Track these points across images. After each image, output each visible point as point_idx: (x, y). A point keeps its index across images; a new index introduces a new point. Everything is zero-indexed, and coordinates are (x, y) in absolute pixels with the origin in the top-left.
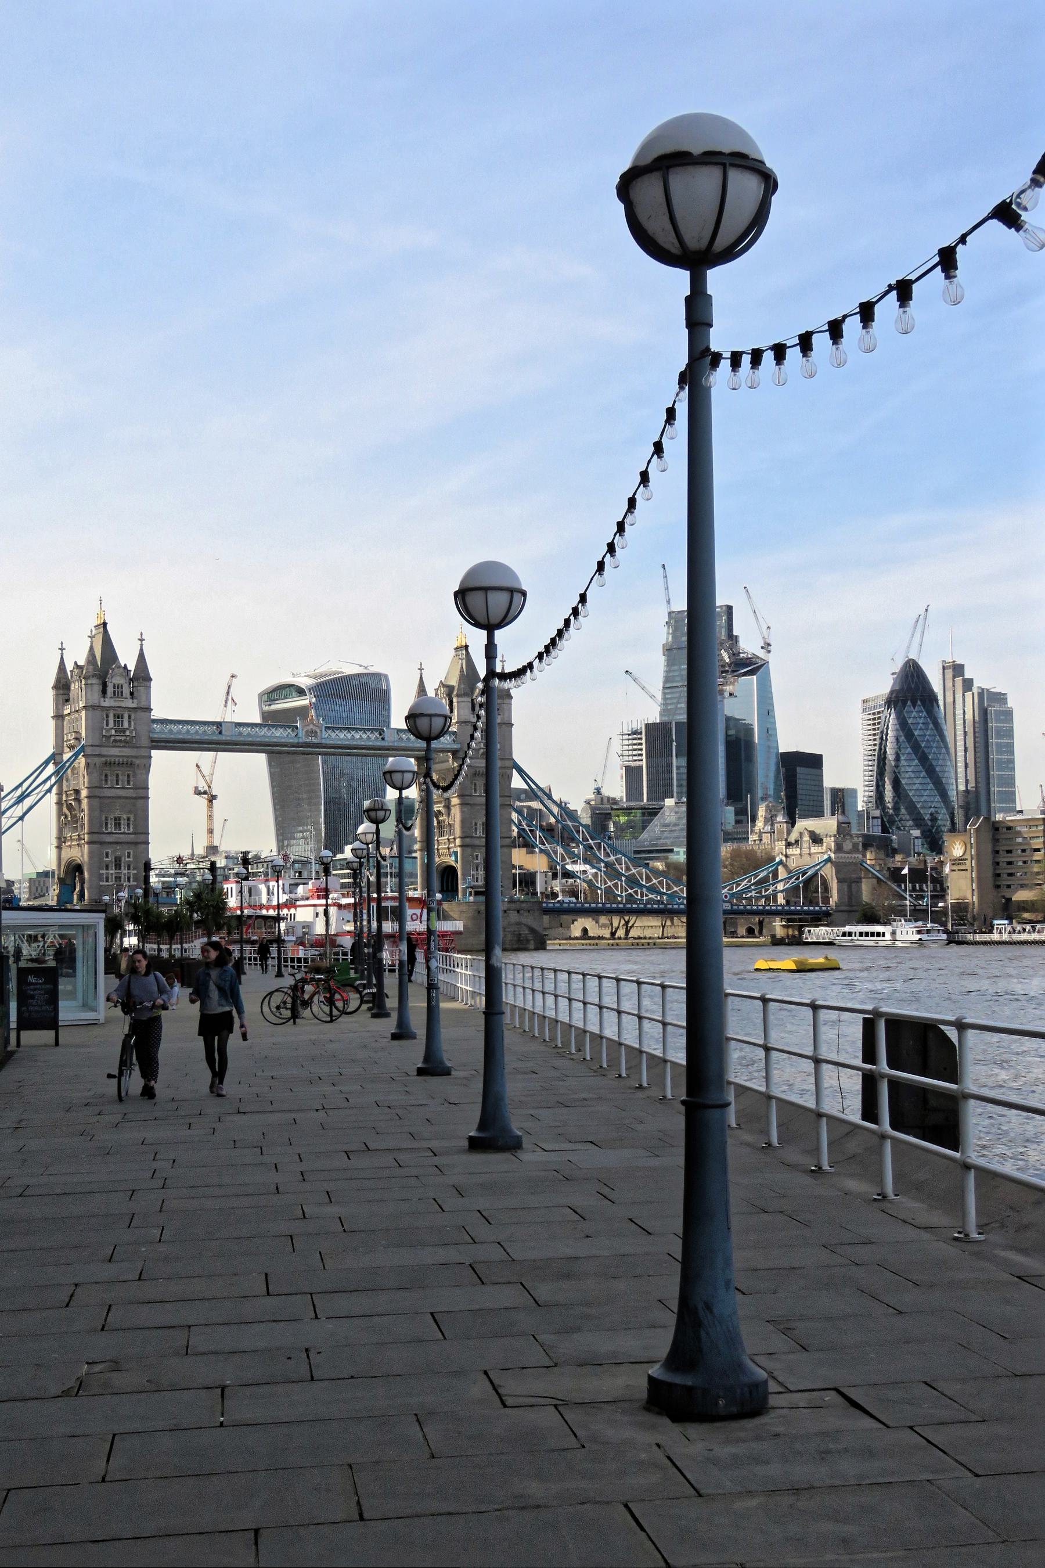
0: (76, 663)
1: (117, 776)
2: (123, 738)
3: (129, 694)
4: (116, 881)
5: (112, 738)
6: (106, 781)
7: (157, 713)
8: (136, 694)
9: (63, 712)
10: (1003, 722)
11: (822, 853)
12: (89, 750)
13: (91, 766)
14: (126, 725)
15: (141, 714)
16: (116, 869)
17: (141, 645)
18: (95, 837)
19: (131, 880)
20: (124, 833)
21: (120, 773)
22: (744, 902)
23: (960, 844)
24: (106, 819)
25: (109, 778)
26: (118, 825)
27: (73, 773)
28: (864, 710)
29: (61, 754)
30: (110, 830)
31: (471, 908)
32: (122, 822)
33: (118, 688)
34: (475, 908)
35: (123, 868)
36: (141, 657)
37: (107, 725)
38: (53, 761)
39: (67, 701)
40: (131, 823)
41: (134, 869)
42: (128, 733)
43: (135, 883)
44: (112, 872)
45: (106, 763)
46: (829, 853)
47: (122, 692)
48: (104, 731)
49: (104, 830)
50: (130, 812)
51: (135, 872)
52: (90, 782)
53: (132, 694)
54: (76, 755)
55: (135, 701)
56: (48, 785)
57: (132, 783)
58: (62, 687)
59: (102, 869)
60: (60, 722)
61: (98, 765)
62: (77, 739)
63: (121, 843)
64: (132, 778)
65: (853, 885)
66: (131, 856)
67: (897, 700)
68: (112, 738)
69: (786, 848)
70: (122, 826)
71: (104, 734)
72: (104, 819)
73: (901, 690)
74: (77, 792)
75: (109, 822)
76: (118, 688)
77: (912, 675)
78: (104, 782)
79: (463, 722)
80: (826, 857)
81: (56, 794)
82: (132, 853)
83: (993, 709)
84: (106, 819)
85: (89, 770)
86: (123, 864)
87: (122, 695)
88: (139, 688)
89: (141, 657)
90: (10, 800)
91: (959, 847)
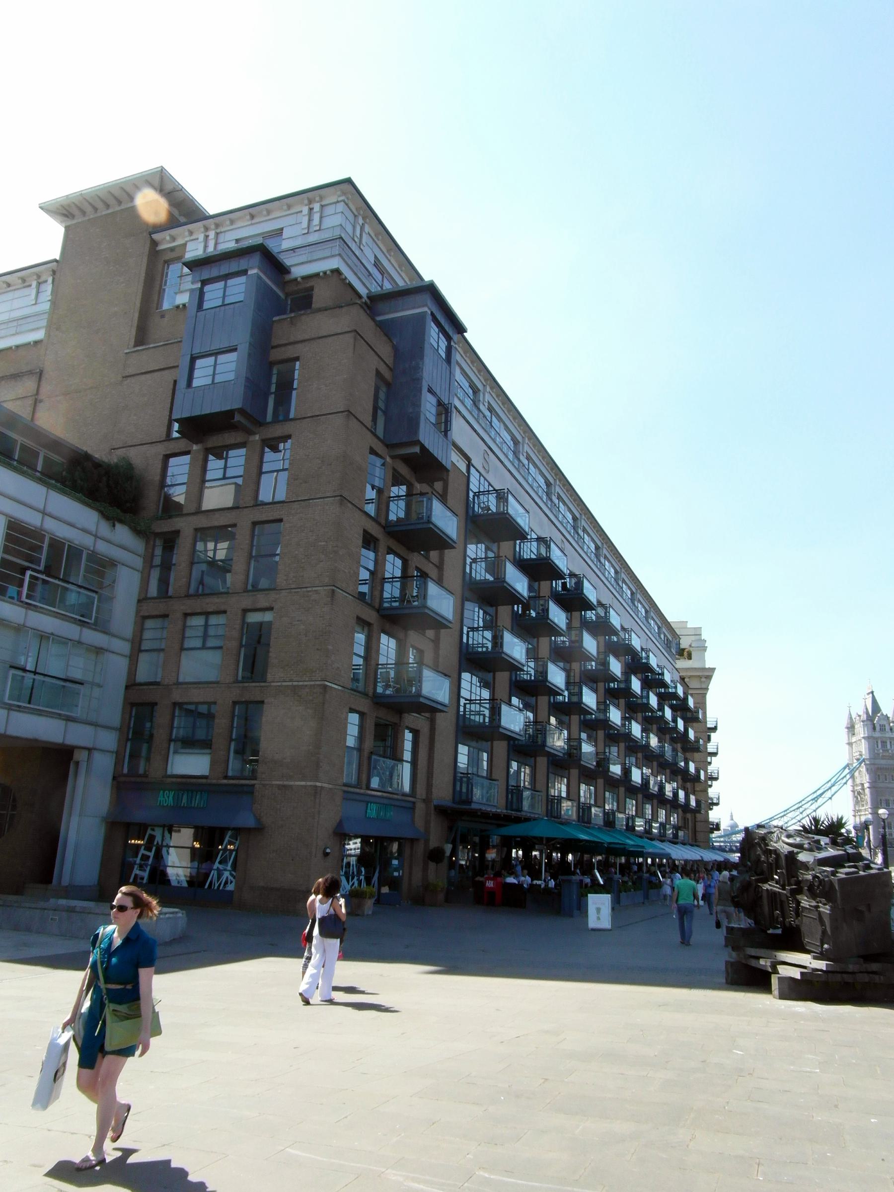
0: (857, 714)
1: (886, 776)
2: (888, 754)
5: (881, 755)
6: (879, 779)
14: (889, 746)
24: (881, 800)
25: (881, 777)
27: (859, 774)
29: (852, 764)
32: (890, 802)
37: (877, 747)
39: (854, 734)
42: (890, 751)
54: (861, 763)
56: (844, 780)
58: (851, 728)
62: (861, 755)
74: (862, 785)
75: (883, 801)
81: (477, 742)
84: (881, 800)
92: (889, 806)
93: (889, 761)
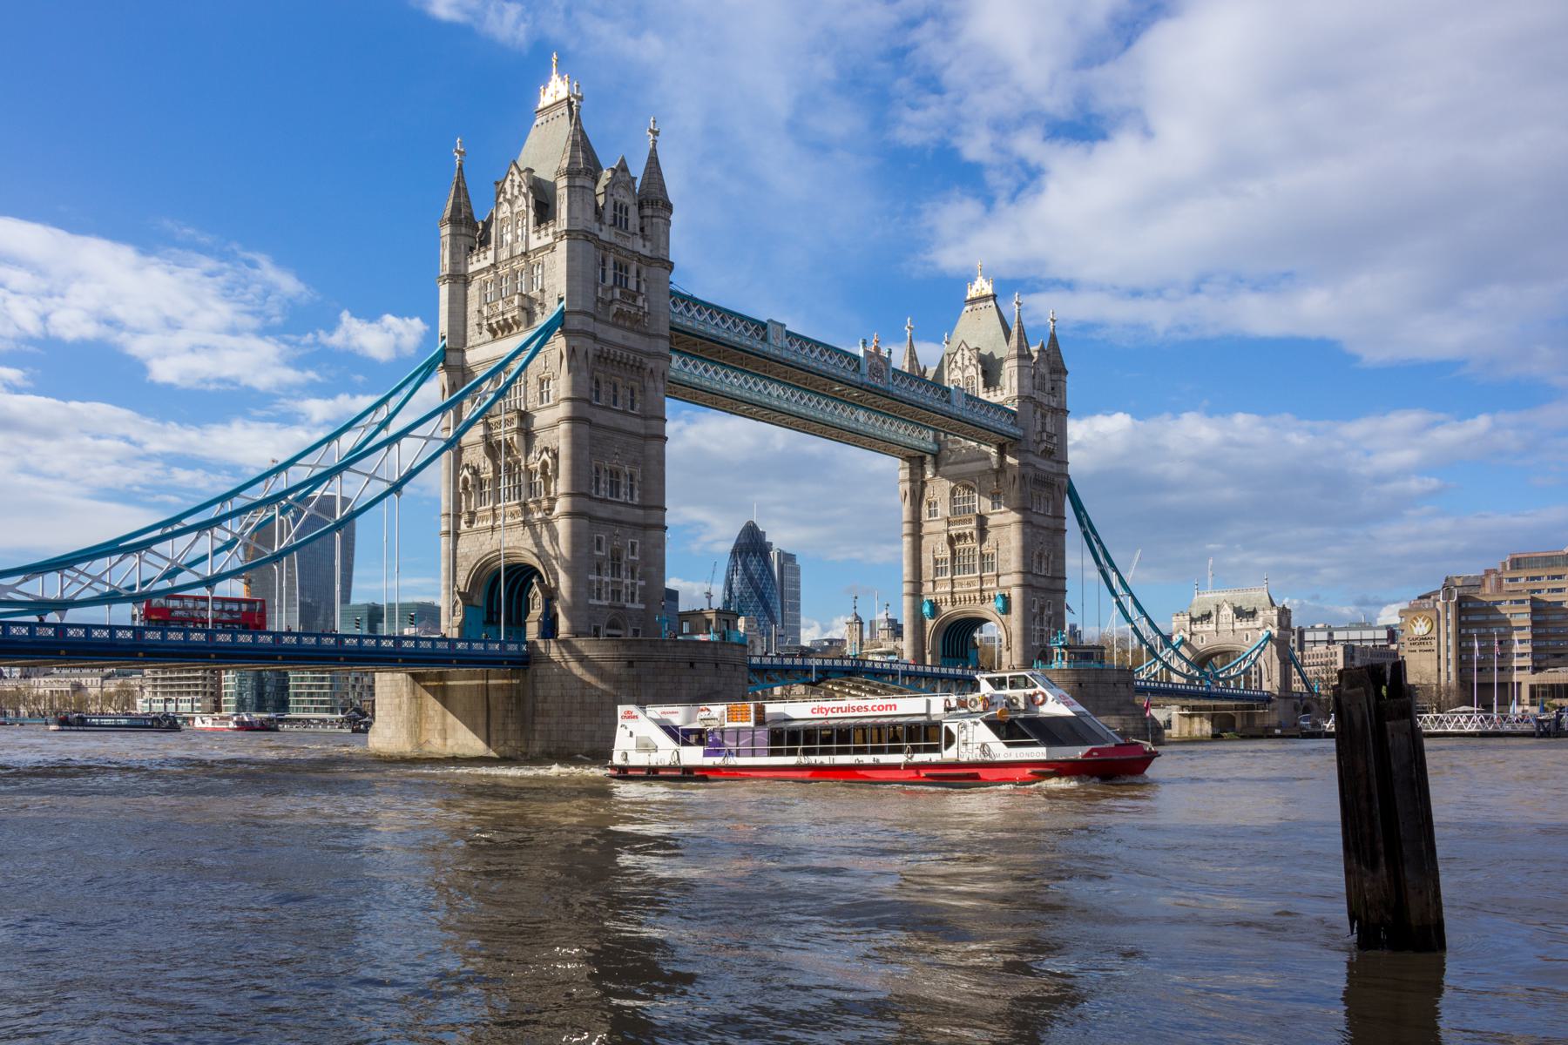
3: (638, 230)
4: (613, 600)
5: (614, 308)
6: (597, 393)
8: (648, 231)
12: (574, 322)
13: (580, 354)
14: (632, 285)
15: (658, 271)
16: (613, 576)
18: (585, 505)
19: (637, 599)
20: (625, 504)
21: (620, 381)
23: (1423, 620)
24: (598, 471)
25: (603, 387)
26: (615, 487)
30: (602, 494)
32: (623, 481)
33: (621, 212)
35: (623, 573)
37: (604, 281)
38: (441, 365)
40: (636, 485)
42: (640, 302)
43: (642, 606)
44: (607, 579)
45: (599, 357)
46: (1269, 628)
47: (627, 220)
48: (600, 289)
49: (593, 491)
50: (635, 463)
51: (643, 583)
52: (575, 386)
53: (642, 229)
55: (648, 244)
57: (638, 406)
60: (459, 287)
64: (638, 397)
66: (637, 550)
68: (614, 308)
70: (622, 490)
71: (600, 294)
76: (621, 212)
79: (1027, 397)
80: (1263, 634)
82: (638, 546)
84: (598, 471)
86: (624, 566)
87: (627, 227)
88: (655, 220)
91: (1423, 624)
92: (618, 496)
93: (632, 336)
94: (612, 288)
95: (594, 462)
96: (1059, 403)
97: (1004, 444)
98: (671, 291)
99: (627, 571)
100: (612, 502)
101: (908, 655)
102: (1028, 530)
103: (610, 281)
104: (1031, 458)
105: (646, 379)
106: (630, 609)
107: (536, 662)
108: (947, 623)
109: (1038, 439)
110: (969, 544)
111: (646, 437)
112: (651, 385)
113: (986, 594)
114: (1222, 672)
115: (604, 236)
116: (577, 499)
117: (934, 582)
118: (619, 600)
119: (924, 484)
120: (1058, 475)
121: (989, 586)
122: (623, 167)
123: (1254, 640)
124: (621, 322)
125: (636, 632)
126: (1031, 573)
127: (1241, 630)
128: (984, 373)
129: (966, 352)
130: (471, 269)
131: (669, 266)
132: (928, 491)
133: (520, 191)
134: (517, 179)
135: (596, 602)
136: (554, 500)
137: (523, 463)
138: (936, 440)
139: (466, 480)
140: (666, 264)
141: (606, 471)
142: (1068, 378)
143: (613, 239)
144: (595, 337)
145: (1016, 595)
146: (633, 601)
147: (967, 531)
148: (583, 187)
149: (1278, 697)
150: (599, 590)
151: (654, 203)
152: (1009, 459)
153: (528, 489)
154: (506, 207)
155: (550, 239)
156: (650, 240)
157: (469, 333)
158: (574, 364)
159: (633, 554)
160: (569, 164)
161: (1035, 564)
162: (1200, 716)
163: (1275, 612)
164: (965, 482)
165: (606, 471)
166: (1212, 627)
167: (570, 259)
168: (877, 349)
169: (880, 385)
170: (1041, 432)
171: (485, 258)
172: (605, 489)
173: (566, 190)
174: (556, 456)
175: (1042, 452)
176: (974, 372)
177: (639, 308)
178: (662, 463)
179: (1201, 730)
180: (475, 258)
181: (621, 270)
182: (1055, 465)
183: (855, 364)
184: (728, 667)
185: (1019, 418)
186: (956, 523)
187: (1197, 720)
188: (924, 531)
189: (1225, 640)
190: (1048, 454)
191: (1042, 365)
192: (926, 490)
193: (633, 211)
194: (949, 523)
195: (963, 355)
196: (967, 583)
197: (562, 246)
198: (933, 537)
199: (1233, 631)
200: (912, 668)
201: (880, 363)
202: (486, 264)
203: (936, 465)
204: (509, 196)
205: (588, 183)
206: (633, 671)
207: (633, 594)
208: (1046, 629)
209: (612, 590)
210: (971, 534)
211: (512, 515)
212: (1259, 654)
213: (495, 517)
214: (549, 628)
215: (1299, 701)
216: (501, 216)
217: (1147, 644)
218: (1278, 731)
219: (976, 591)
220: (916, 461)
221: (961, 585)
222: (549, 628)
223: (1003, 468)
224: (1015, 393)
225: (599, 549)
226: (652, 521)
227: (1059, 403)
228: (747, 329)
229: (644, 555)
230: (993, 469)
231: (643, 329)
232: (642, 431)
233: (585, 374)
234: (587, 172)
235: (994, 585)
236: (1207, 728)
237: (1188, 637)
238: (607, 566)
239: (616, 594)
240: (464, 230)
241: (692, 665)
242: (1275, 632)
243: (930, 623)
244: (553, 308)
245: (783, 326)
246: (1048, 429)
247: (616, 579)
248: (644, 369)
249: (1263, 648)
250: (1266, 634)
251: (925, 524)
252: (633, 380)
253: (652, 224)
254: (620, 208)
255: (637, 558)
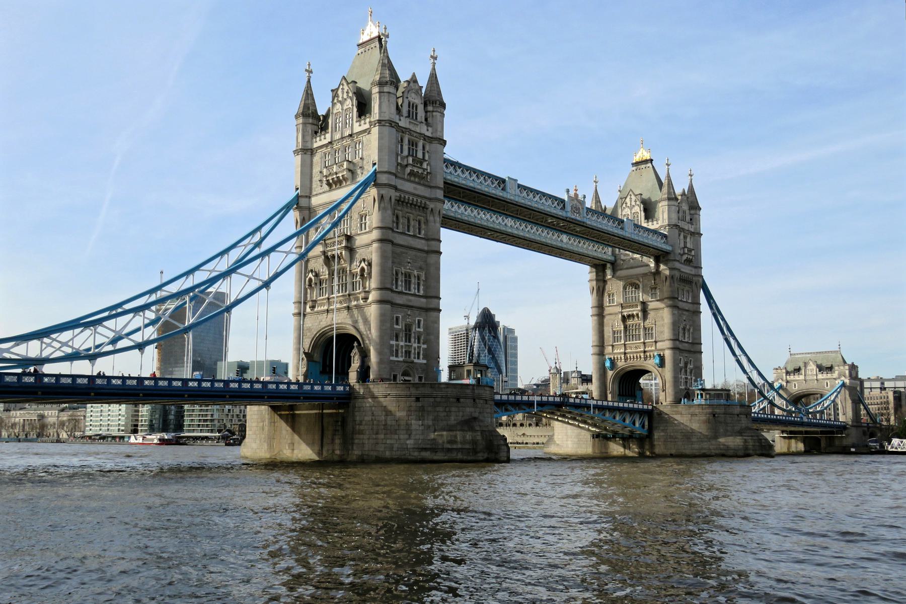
4: (406, 357)
5: (408, 170)
6: (397, 224)
7: (450, 152)
8: (430, 120)
9: (312, 144)
10: (513, 342)
11: (834, 379)
12: (383, 179)
13: (387, 199)
14: (420, 155)
15: (436, 146)
16: (406, 341)
17: (434, 64)
18: (389, 296)
19: (421, 356)
20: (414, 295)
22: (810, 416)
24: (397, 274)
25: (401, 220)
26: (408, 283)
28: (450, 333)
31: (705, 411)
32: (413, 280)
33: (413, 108)
34: (710, 411)
35: (413, 340)
36: (433, 78)
37: (402, 152)
38: (295, 206)
40: (422, 283)
41: (423, 344)
42: (425, 165)
43: (425, 362)
45: (398, 201)
46: (843, 378)
47: (416, 114)
48: (399, 158)
49: (394, 287)
50: (421, 268)
51: (425, 346)
52: (383, 219)
53: (426, 120)
55: (430, 129)
57: (423, 232)
59: (393, 340)
60: (308, 156)
61: (393, 200)
63: (412, 307)
64: (423, 226)
65: (857, 405)
66: (422, 325)
67: (480, 326)
68: (408, 170)
69: (786, 375)
70: (412, 286)
71: (399, 161)
72: (394, 272)
73: (482, 322)
76: (413, 108)
77: (487, 316)
78: (395, 225)
80: (839, 382)
82: (422, 323)
83: (509, 336)
84: (397, 274)
85: (382, 205)
86: (413, 335)
87: (416, 118)
88: (434, 113)
89: (433, 78)
90: (245, 246)
92: (410, 290)
93: (418, 187)
94: (407, 157)
95: (395, 268)
96: (695, 229)
97: (659, 256)
98: (445, 159)
99: (415, 338)
100: (406, 294)
101: (595, 394)
102: (676, 312)
103: (406, 153)
104: (677, 265)
105: (428, 215)
106: (416, 363)
107: (356, 398)
108: (622, 373)
109: (682, 252)
110: (636, 321)
111: (427, 252)
112: (431, 218)
113: (648, 354)
114: (811, 408)
115: (402, 124)
116: (384, 292)
117: (613, 346)
118: (410, 357)
119: (605, 282)
120: (695, 275)
121: (650, 349)
122: (414, 80)
123: (832, 387)
124: (412, 179)
125: (420, 378)
126: (678, 340)
127: (823, 379)
128: (645, 210)
129: (633, 197)
130: (315, 145)
131: (444, 143)
132: (609, 287)
133: (348, 95)
134: (346, 88)
135: (394, 358)
136: (368, 292)
137: (348, 269)
138: (613, 254)
139: (310, 280)
140: (441, 142)
141: (402, 273)
142: (701, 212)
143: (407, 126)
144: (396, 188)
145: (668, 354)
146: (418, 358)
147: (635, 313)
148: (389, 93)
149: (852, 426)
150: (397, 351)
151: (433, 103)
152: (662, 267)
153: (351, 286)
154: (338, 106)
155: (367, 126)
156: (431, 127)
157: (314, 186)
158: (382, 205)
159: (419, 327)
160: (380, 78)
161: (681, 335)
162: (795, 438)
163: (847, 367)
164: (632, 284)
165: (402, 273)
166: (802, 377)
167: (381, 138)
168: (576, 195)
169: (578, 219)
170: (684, 248)
171: (325, 138)
172: (402, 286)
173: (378, 95)
174: (370, 265)
175: (685, 261)
176: (638, 209)
177: (424, 170)
178: (438, 269)
179: (796, 448)
180: (318, 139)
181: (413, 146)
182: (693, 269)
183: (562, 205)
184: (482, 401)
185: (669, 239)
186: (626, 307)
187: (793, 441)
188: (606, 312)
189: (812, 386)
190: (688, 262)
191: (684, 204)
192: (607, 287)
193: (421, 108)
194: (622, 307)
195: (631, 198)
196: (635, 346)
197: (375, 130)
198: (612, 317)
199: (817, 380)
200: (600, 403)
201: (578, 204)
202: (325, 142)
203: (614, 270)
204: (340, 99)
205: (392, 90)
206: (419, 404)
207: (419, 353)
208: (689, 377)
209: (406, 351)
210: (637, 315)
211: (341, 302)
212: (836, 396)
213: (329, 304)
214: (364, 374)
215: (866, 429)
216: (335, 111)
217: (758, 388)
218: (853, 450)
219: (641, 352)
220: (599, 267)
221: (631, 348)
222: (364, 374)
223: (657, 273)
224: (666, 222)
225: (397, 324)
226: (432, 306)
227: (695, 229)
228: (493, 183)
229: (426, 328)
230: (651, 273)
231: (427, 183)
232: (426, 248)
233: (389, 212)
234: (392, 83)
235: (653, 348)
236: (801, 446)
237: (784, 384)
238: (402, 335)
239: (408, 353)
240: (311, 120)
241: (458, 400)
242: (847, 381)
243: (610, 373)
244: (369, 170)
245: (516, 180)
246: (688, 245)
247: (408, 344)
248: (427, 209)
249: (839, 392)
250: (841, 383)
251: (606, 308)
252: (421, 216)
253: (433, 116)
254: (412, 106)
255: (422, 330)
